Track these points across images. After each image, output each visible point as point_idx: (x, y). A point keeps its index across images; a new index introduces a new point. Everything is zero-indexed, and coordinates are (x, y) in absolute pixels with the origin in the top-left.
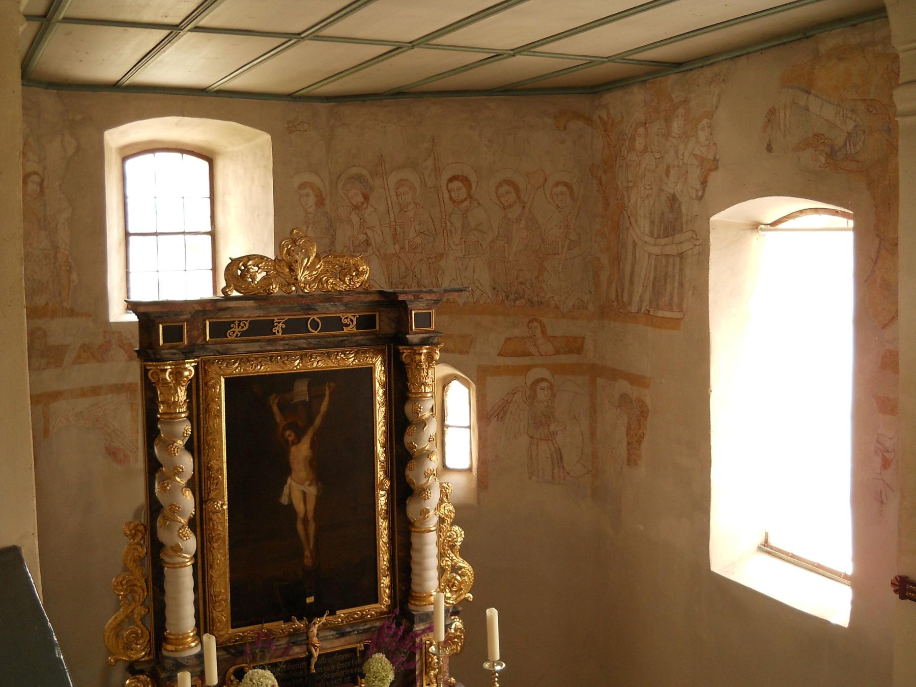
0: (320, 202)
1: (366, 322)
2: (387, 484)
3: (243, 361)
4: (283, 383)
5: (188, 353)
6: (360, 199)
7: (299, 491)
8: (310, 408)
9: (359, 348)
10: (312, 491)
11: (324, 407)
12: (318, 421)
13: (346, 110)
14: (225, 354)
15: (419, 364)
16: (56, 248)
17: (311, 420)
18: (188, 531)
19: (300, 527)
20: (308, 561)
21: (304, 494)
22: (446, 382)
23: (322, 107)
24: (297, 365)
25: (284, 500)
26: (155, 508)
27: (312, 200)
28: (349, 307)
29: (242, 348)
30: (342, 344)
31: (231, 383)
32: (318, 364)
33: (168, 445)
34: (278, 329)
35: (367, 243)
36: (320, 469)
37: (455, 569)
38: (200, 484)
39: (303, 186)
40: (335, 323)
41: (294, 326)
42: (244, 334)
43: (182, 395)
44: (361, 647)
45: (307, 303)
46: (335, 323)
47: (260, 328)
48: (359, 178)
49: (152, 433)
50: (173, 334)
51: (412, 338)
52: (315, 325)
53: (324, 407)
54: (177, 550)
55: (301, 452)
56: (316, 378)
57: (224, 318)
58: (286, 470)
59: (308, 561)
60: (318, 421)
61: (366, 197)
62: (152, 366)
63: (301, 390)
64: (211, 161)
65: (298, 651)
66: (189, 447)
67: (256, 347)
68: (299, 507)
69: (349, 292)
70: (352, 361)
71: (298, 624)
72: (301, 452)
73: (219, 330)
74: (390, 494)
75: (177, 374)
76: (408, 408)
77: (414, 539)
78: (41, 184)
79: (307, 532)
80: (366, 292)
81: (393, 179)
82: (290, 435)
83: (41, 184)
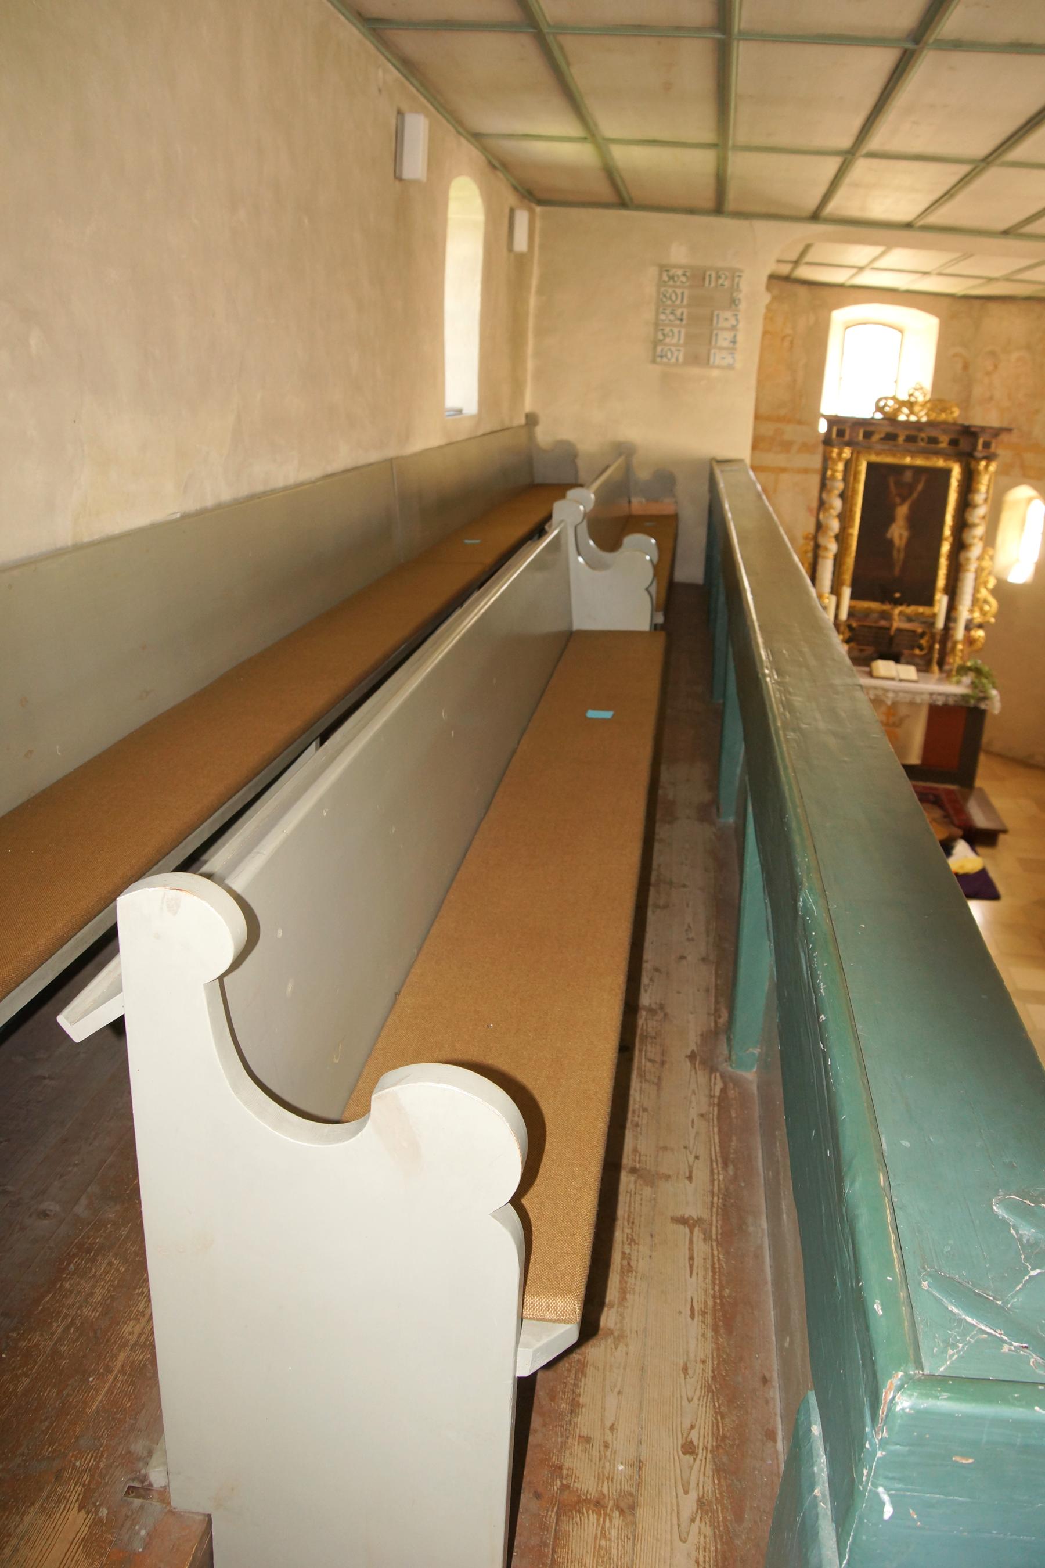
0: (966, 367)
1: (954, 443)
2: (951, 540)
3: (878, 454)
4: (899, 469)
5: (848, 444)
6: (990, 368)
7: (898, 532)
8: (911, 487)
9: (947, 456)
10: (906, 534)
11: (920, 487)
12: (915, 495)
13: (992, 306)
14: (869, 449)
15: (979, 473)
16: (795, 381)
17: (910, 494)
18: (833, 540)
19: (895, 553)
20: (897, 571)
21: (901, 536)
22: (1030, 500)
23: (977, 303)
24: (908, 460)
25: (889, 536)
26: (819, 526)
27: (959, 366)
28: (944, 432)
29: (879, 447)
30: (937, 453)
31: (870, 466)
32: (920, 462)
33: (830, 492)
34: (901, 439)
35: (991, 398)
36: (913, 522)
37: (986, 602)
38: (845, 517)
39: (956, 355)
40: (933, 440)
41: (911, 439)
42: (882, 439)
43: (840, 466)
44: (920, 630)
45: (918, 426)
46: (933, 440)
47: (891, 437)
48: (993, 354)
49: (823, 486)
50: (841, 433)
51: (978, 454)
52: (922, 440)
53: (920, 487)
54: (826, 549)
55: (902, 511)
56: (918, 470)
57: (870, 429)
58: (891, 519)
59: (897, 571)
60: (915, 495)
61: (996, 367)
62: (828, 448)
63: (908, 476)
64: (901, 331)
65: (883, 623)
66: (842, 496)
67: (886, 447)
68: (897, 541)
69: (945, 423)
70: (940, 463)
71: (886, 607)
72: (902, 511)
73: (868, 435)
74: (953, 546)
75: (840, 454)
76: (970, 496)
77: (961, 575)
78: (792, 342)
79: (898, 557)
80: (955, 424)
81: (1015, 356)
82: (898, 500)
83: (792, 342)
